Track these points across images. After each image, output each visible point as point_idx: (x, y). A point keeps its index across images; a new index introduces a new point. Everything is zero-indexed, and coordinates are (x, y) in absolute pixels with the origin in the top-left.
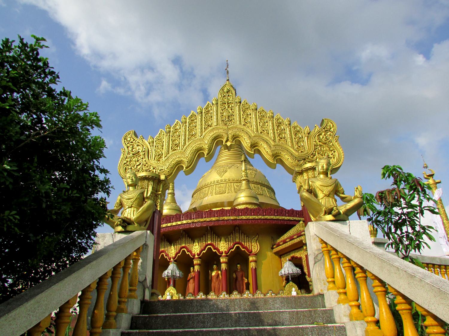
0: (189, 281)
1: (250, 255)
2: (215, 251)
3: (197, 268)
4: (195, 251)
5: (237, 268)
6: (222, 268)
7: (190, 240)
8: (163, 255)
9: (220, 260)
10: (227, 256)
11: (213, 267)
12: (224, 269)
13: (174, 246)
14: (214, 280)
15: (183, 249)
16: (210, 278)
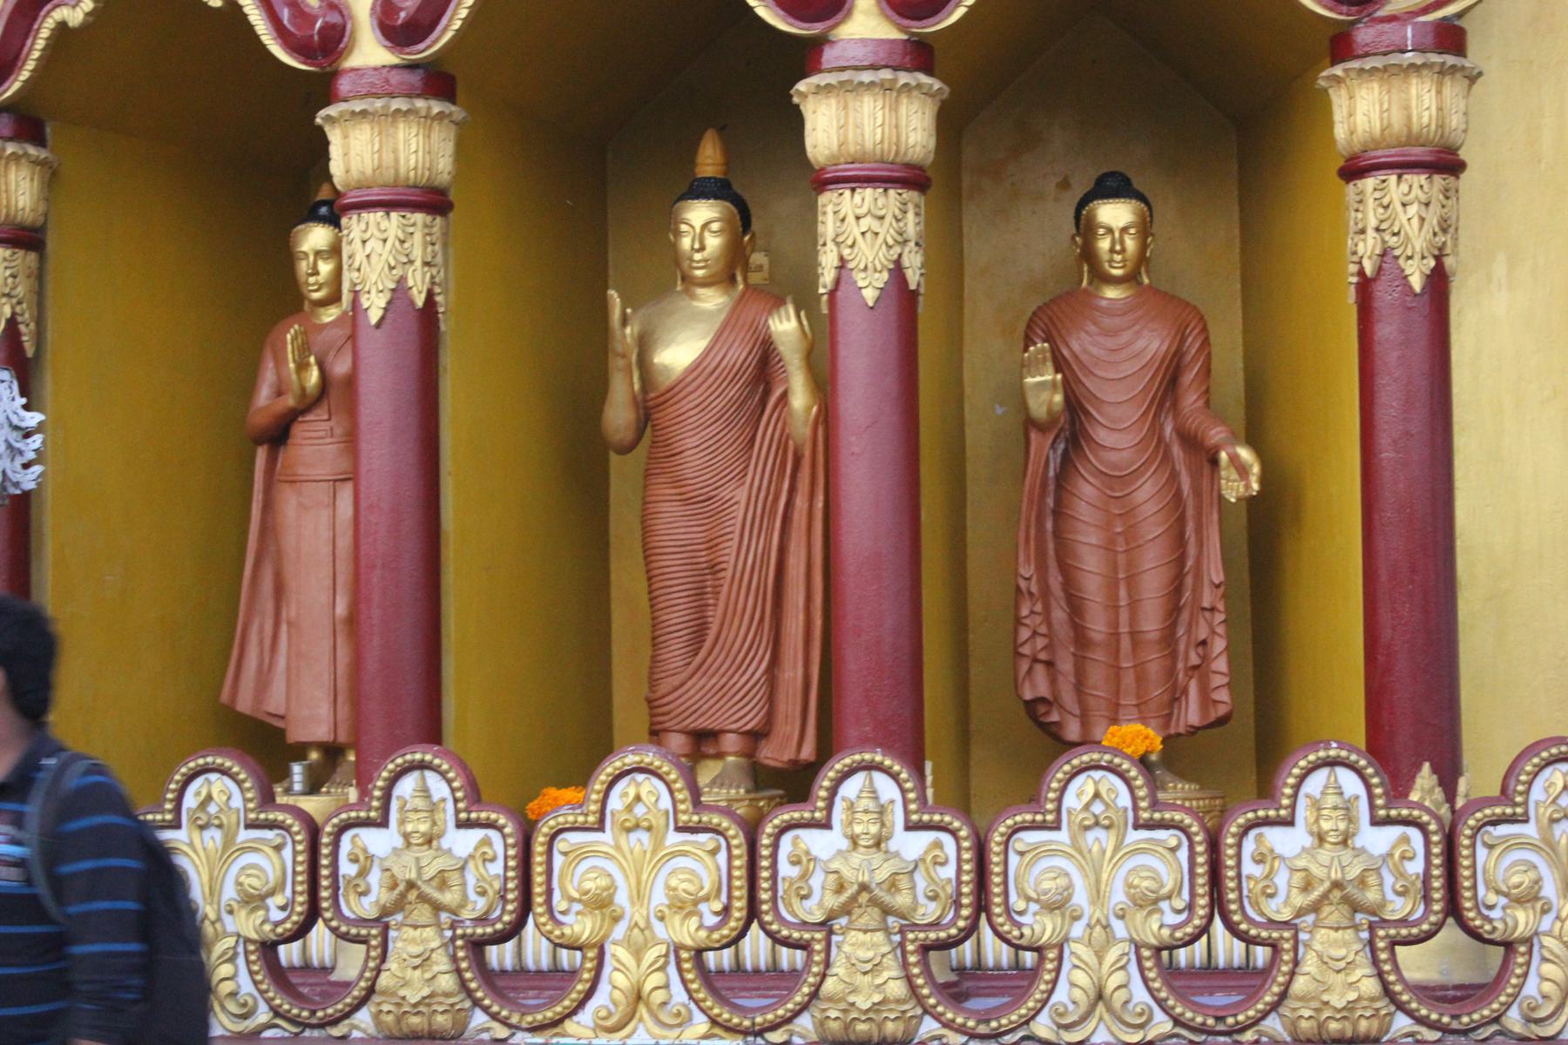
0: (278, 434)
1: (1341, 47)
3: (372, 261)
5: (1088, 254)
9: (795, 121)
10: (920, 55)
11: (669, 223)
12: (870, 287)
14: (698, 442)
16: (619, 415)
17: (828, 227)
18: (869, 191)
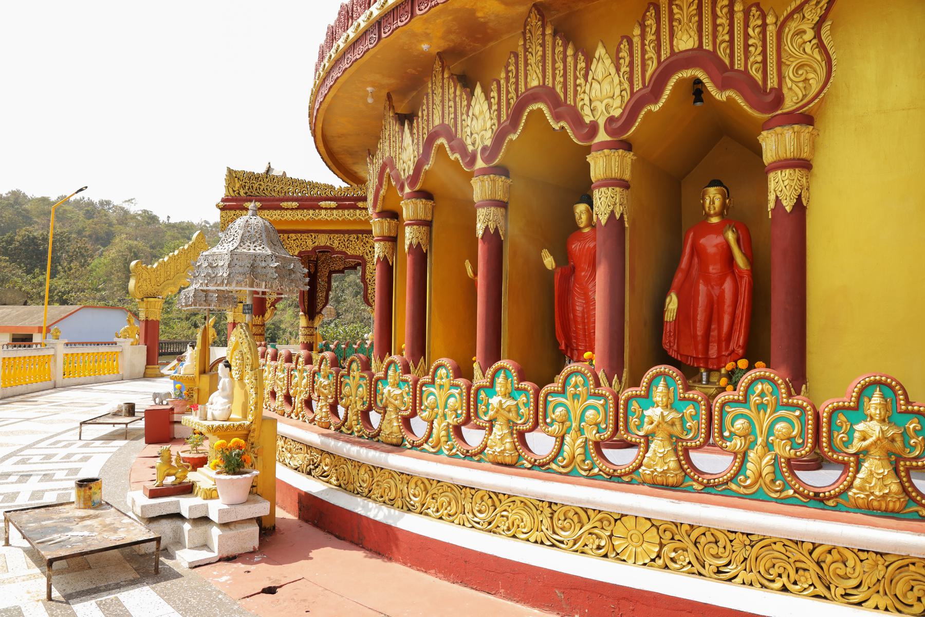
2: (728, 98)
3: (605, 203)
4: (597, 114)
6: (772, 197)
7: (570, 52)
8: (442, 145)
13: (488, 98)
15: (535, 107)
17: (772, 185)
18: (788, 171)
